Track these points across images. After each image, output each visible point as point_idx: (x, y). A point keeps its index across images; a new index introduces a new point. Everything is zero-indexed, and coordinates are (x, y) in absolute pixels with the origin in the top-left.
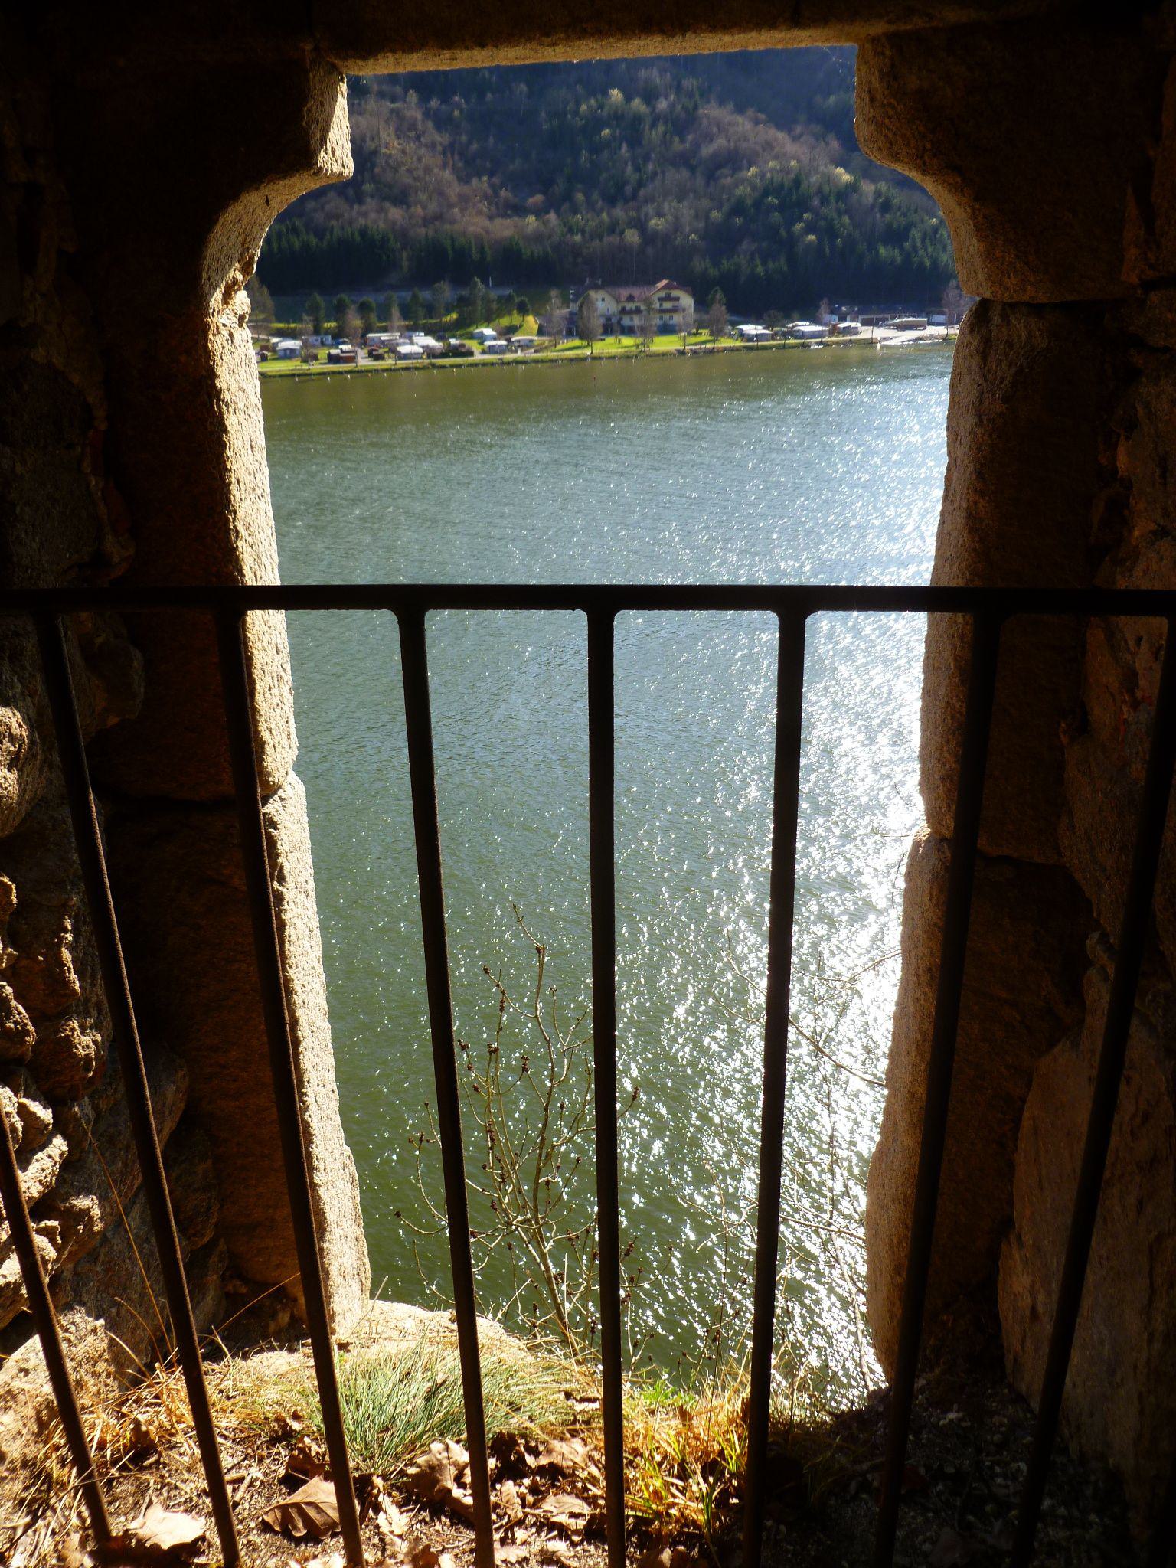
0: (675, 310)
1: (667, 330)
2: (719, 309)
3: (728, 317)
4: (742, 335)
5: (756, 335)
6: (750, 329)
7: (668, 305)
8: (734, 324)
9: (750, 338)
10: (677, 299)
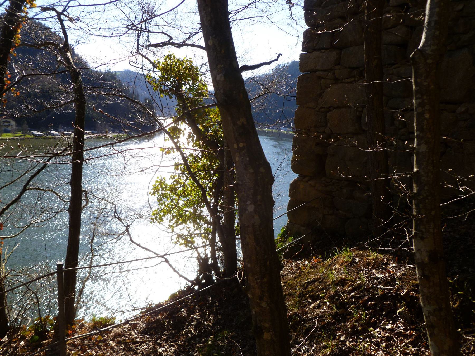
0: (9, 125)
1: (7, 132)
2: (25, 126)
3: (29, 129)
4: (33, 134)
5: (38, 134)
6: (36, 132)
7: (6, 124)
8: (30, 131)
9: (36, 135)
10: (9, 122)
